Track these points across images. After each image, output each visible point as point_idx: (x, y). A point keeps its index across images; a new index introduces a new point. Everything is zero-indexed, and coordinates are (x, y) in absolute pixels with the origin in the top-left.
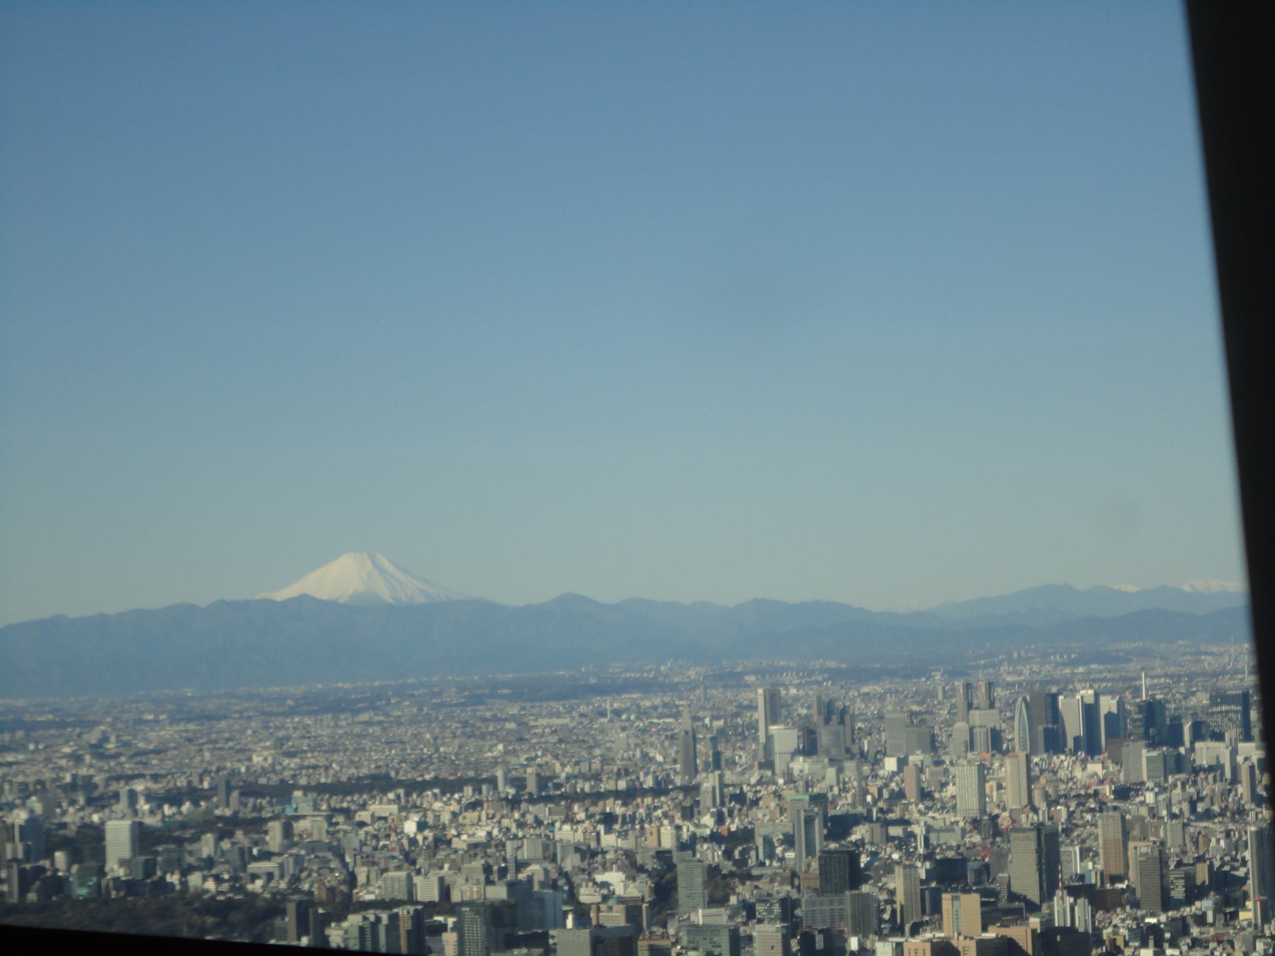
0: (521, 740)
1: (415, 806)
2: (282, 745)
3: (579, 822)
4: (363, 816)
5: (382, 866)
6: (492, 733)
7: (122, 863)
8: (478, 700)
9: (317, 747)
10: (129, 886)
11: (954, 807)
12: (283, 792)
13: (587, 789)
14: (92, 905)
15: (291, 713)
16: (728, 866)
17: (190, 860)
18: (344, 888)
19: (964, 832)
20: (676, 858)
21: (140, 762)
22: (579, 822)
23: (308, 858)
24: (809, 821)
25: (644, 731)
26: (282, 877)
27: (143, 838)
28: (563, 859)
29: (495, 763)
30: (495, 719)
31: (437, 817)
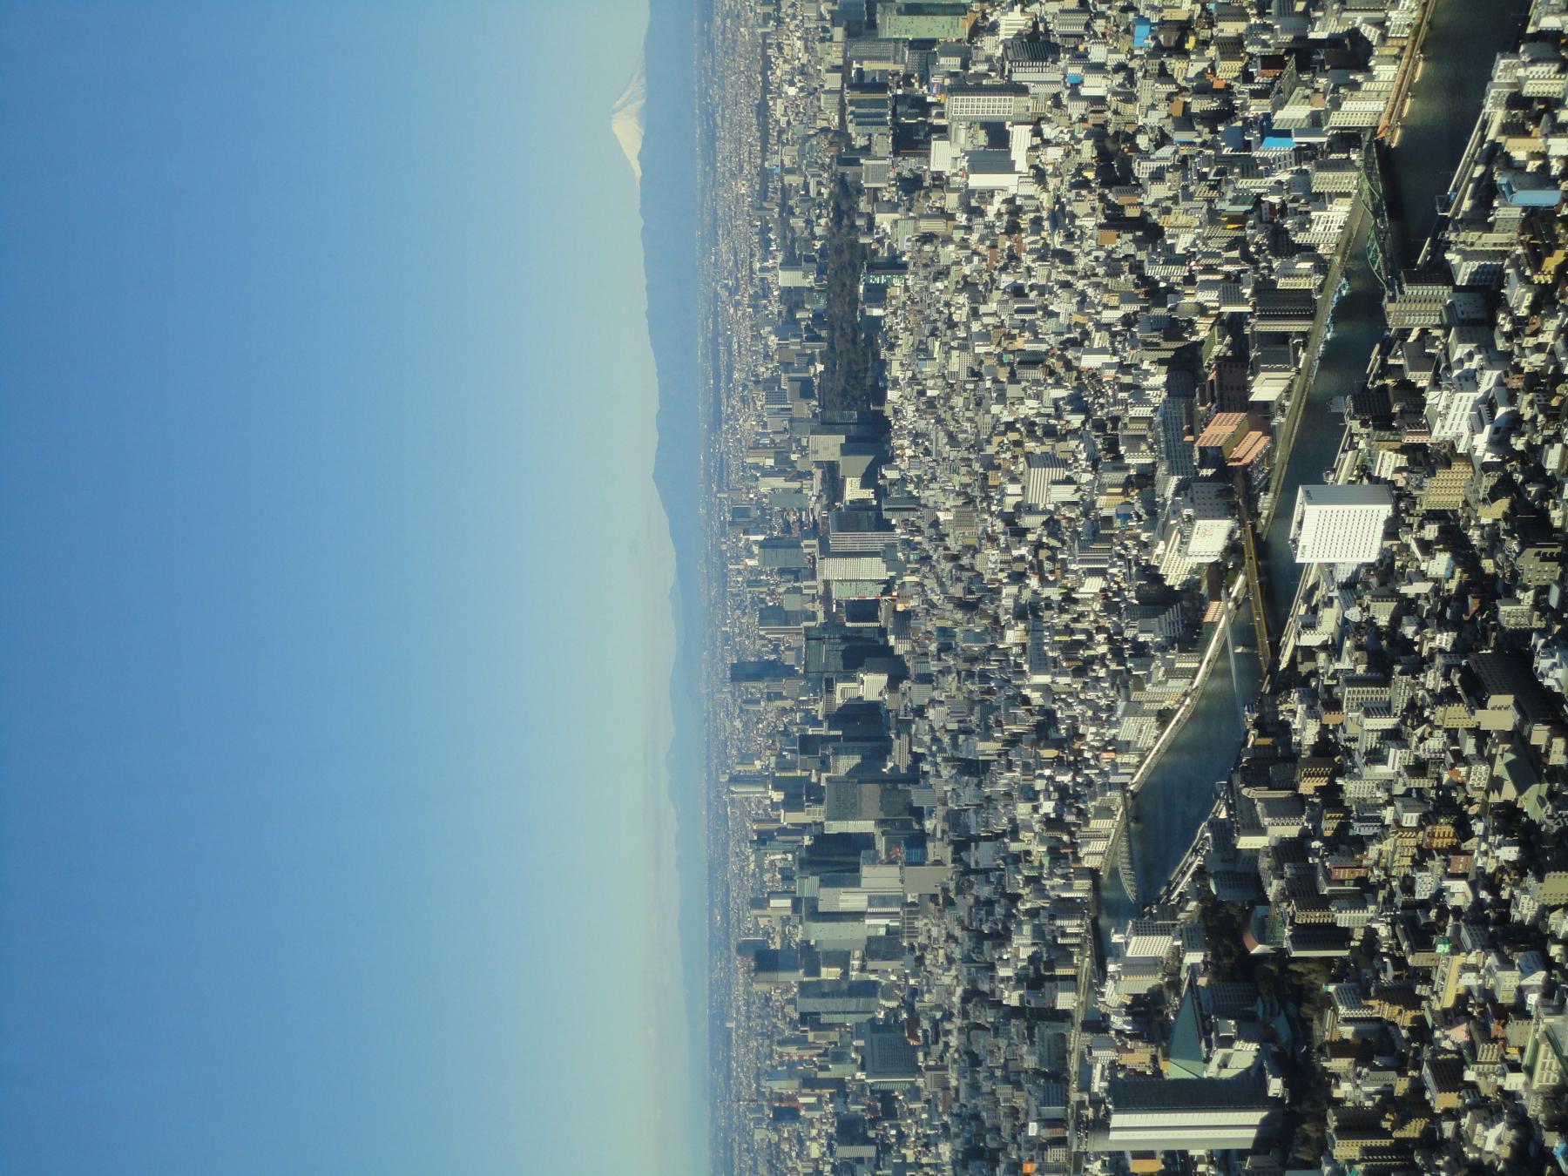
0: (738, 16)
1: (778, 88)
4: (783, 121)
7: (805, 277)
9: (737, 152)
10: (821, 272)
12: (765, 175)
17: (806, 233)
18: (830, 136)
26: (820, 176)
27: (790, 263)
29: (753, 34)
30: (723, 33)
31: (786, 73)
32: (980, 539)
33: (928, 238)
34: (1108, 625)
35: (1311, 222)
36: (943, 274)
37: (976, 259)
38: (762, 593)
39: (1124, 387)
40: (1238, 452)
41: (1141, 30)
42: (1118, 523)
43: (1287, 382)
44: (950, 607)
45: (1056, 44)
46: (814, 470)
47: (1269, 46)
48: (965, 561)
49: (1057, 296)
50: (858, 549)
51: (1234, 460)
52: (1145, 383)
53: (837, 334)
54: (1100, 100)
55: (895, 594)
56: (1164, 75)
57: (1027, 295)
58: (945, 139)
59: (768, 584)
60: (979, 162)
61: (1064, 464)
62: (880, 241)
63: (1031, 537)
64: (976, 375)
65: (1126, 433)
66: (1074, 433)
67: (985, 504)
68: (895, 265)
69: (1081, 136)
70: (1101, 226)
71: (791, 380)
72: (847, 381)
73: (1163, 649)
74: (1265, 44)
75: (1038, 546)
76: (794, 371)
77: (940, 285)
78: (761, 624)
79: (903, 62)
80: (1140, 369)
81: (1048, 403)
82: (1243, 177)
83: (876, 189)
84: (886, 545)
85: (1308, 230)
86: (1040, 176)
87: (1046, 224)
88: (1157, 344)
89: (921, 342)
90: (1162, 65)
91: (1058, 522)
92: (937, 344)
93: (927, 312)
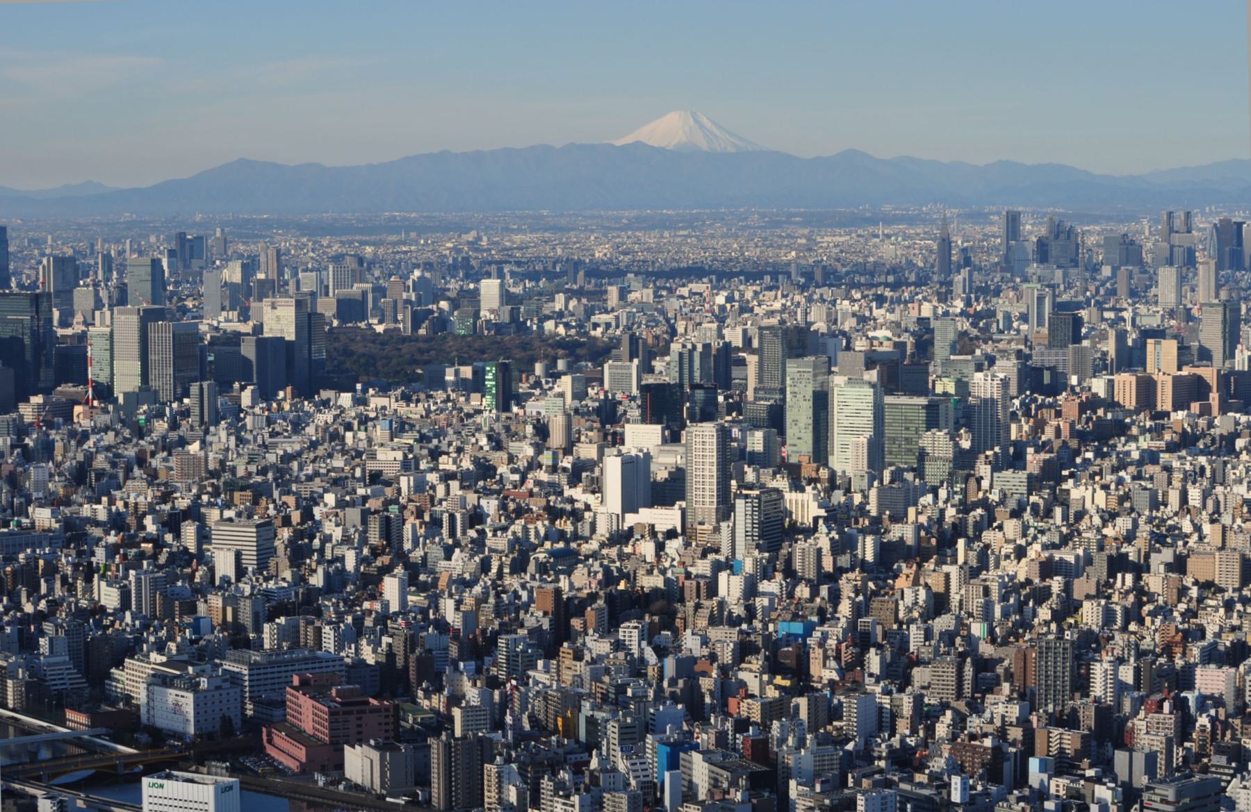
0: (810, 250)
2: (618, 247)
3: (855, 301)
5: (698, 321)
6: (787, 246)
7: (492, 311)
8: (776, 224)
10: (499, 328)
11: (1156, 303)
12: (617, 274)
13: (863, 280)
14: (470, 339)
15: (625, 228)
16: (975, 332)
17: (547, 312)
18: (665, 336)
19: (1163, 317)
20: (933, 324)
21: (508, 255)
22: (855, 301)
23: (637, 315)
24: (1041, 299)
25: (908, 247)
28: (842, 324)
30: (789, 236)
32: (166, 484)
33: (542, 431)
34: (62, 615)
35: (567, 797)
36: (497, 445)
37: (516, 477)
38: (96, 273)
39: (358, 622)
40: (280, 739)
41: (798, 628)
42: (188, 619)
43: (367, 784)
44: (80, 457)
45: (780, 548)
46: (251, 323)
47: (779, 746)
48: (137, 472)
49: (472, 557)
50: (152, 357)
51: (269, 734)
52: (364, 642)
53: (421, 345)
54: (712, 590)
55: (96, 403)
56: (744, 650)
57: (471, 527)
58: (665, 441)
59: (107, 279)
60: (635, 468)
61: (262, 565)
62: (537, 384)
63: (169, 538)
64: (375, 478)
65: (302, 623)
66: (300, 580)
67: (210, 489)
68: (507, 398)
69: (669, 574)
70: (558, 592)
71: (364, 294)
72: (364, 355)
73: (31, 669)
74: (783, 741)
75: (158, 543)
76: (375, 301)
77: (484, 441)
78: (56, 259)
79: (756, 399)
80: (382, 634)
81: (338, 552)
82: (621, 728)
83: (601, 382)
84: (156, 392)
85: (556, 794)
86: (621, 537)
87: (561, 545)
88: (413, 651)
89: (414, 426)
90: (756, 651)
91: (189, 564)
92: (411, 442)
93: (450, 431)
